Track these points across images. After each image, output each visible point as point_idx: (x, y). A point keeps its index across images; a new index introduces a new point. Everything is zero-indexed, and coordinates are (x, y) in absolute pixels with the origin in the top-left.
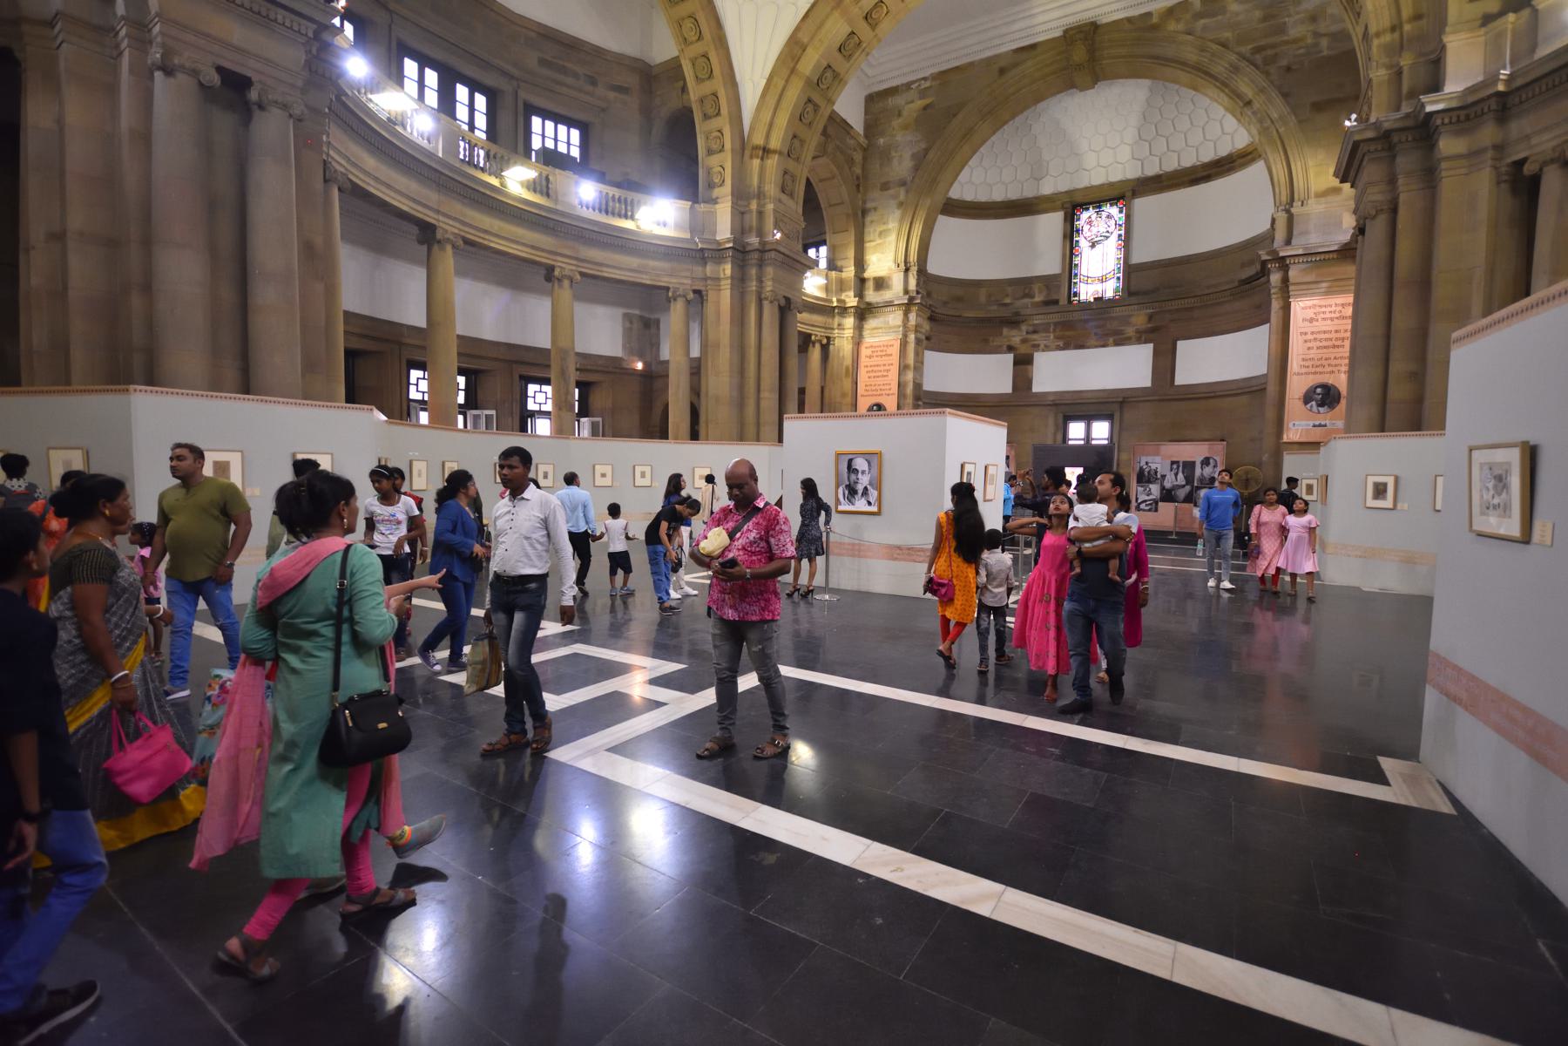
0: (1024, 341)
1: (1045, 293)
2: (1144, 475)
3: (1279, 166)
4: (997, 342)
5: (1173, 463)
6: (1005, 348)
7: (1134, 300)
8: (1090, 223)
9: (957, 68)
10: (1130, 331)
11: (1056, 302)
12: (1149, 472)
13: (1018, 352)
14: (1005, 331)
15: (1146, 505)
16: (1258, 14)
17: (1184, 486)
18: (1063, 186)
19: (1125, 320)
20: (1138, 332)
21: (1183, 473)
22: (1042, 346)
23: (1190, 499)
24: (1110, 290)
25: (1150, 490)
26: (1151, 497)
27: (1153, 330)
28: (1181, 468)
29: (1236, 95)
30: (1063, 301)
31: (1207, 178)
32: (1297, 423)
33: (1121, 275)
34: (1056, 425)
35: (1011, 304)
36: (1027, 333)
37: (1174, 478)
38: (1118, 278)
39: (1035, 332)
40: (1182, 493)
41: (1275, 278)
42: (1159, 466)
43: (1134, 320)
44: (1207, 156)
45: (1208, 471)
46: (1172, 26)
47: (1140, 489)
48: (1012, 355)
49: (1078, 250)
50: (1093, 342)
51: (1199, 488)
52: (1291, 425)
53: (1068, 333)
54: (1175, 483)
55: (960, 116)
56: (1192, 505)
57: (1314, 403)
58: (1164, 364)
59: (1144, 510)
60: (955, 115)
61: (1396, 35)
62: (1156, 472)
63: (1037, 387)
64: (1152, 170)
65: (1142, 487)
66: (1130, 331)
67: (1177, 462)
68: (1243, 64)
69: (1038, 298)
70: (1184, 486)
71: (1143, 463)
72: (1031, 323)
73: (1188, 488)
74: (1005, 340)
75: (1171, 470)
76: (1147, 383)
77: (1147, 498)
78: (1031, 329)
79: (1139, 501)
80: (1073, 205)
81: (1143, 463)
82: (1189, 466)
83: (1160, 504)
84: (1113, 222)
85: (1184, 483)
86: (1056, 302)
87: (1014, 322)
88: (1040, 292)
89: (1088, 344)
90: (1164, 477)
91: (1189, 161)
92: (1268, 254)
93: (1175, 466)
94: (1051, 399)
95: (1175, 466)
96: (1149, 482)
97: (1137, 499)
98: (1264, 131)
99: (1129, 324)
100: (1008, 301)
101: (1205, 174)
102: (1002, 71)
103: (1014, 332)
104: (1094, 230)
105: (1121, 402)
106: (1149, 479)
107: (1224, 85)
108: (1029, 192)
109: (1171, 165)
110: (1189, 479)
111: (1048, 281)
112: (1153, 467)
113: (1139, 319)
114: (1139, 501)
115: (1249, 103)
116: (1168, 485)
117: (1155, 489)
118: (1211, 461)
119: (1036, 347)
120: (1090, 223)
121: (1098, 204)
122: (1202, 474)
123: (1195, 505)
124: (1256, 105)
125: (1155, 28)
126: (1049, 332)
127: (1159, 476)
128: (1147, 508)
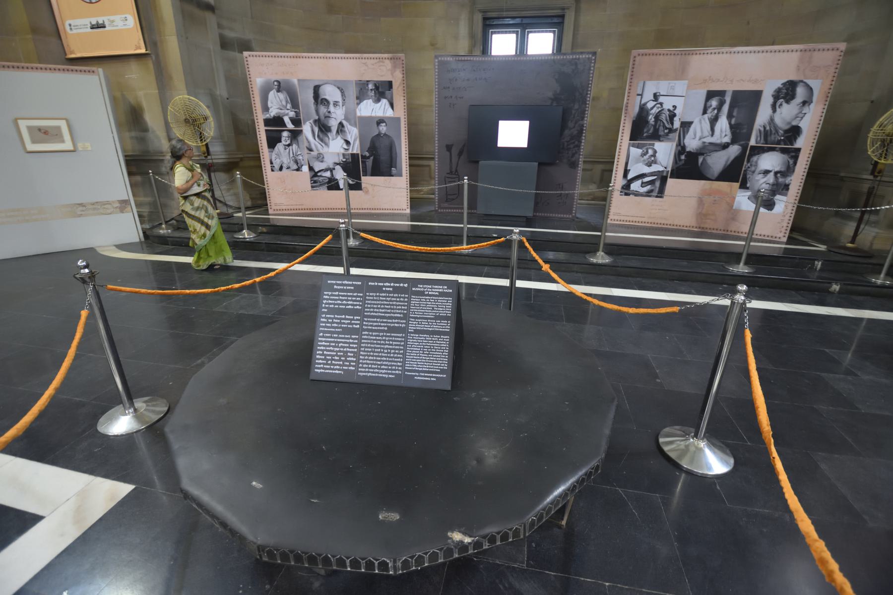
2: (647, 122)
5: (711, 95)
12: (657, 117)
15: (643, 185)
17: (725, 146)
21: (730, 116)
25: (655, 152)
26: (655, 168)
28: (726, 108)
34: (472, 36)
37: (707, 125)
40: (718, 162)
42: (679, 102)
45: (786, 113)
47: (635, 152)
51: (757, 151)
56: (737, 185)
59: (637, 194)
62: (672, 116)
65: (638, 147)
67: (721, 94)
70: (725, 146)
71: (648, 96)
75: (705, 112)
77: (646, 170)
79: (630, 176)
83: (670, 182)
85: (727, 139)
90: (686, 125)
93: (714, 103)
95: (714, 103)
97: (626, 172)
106: (656, 130)
110: (739, 133)
112: (668, 103)
114: (630, 176)
116: (692, 143)
118: (800, 91)
122: (772, 120)
123: (744, 186)
127: (677, 124)
128: (648, 188)
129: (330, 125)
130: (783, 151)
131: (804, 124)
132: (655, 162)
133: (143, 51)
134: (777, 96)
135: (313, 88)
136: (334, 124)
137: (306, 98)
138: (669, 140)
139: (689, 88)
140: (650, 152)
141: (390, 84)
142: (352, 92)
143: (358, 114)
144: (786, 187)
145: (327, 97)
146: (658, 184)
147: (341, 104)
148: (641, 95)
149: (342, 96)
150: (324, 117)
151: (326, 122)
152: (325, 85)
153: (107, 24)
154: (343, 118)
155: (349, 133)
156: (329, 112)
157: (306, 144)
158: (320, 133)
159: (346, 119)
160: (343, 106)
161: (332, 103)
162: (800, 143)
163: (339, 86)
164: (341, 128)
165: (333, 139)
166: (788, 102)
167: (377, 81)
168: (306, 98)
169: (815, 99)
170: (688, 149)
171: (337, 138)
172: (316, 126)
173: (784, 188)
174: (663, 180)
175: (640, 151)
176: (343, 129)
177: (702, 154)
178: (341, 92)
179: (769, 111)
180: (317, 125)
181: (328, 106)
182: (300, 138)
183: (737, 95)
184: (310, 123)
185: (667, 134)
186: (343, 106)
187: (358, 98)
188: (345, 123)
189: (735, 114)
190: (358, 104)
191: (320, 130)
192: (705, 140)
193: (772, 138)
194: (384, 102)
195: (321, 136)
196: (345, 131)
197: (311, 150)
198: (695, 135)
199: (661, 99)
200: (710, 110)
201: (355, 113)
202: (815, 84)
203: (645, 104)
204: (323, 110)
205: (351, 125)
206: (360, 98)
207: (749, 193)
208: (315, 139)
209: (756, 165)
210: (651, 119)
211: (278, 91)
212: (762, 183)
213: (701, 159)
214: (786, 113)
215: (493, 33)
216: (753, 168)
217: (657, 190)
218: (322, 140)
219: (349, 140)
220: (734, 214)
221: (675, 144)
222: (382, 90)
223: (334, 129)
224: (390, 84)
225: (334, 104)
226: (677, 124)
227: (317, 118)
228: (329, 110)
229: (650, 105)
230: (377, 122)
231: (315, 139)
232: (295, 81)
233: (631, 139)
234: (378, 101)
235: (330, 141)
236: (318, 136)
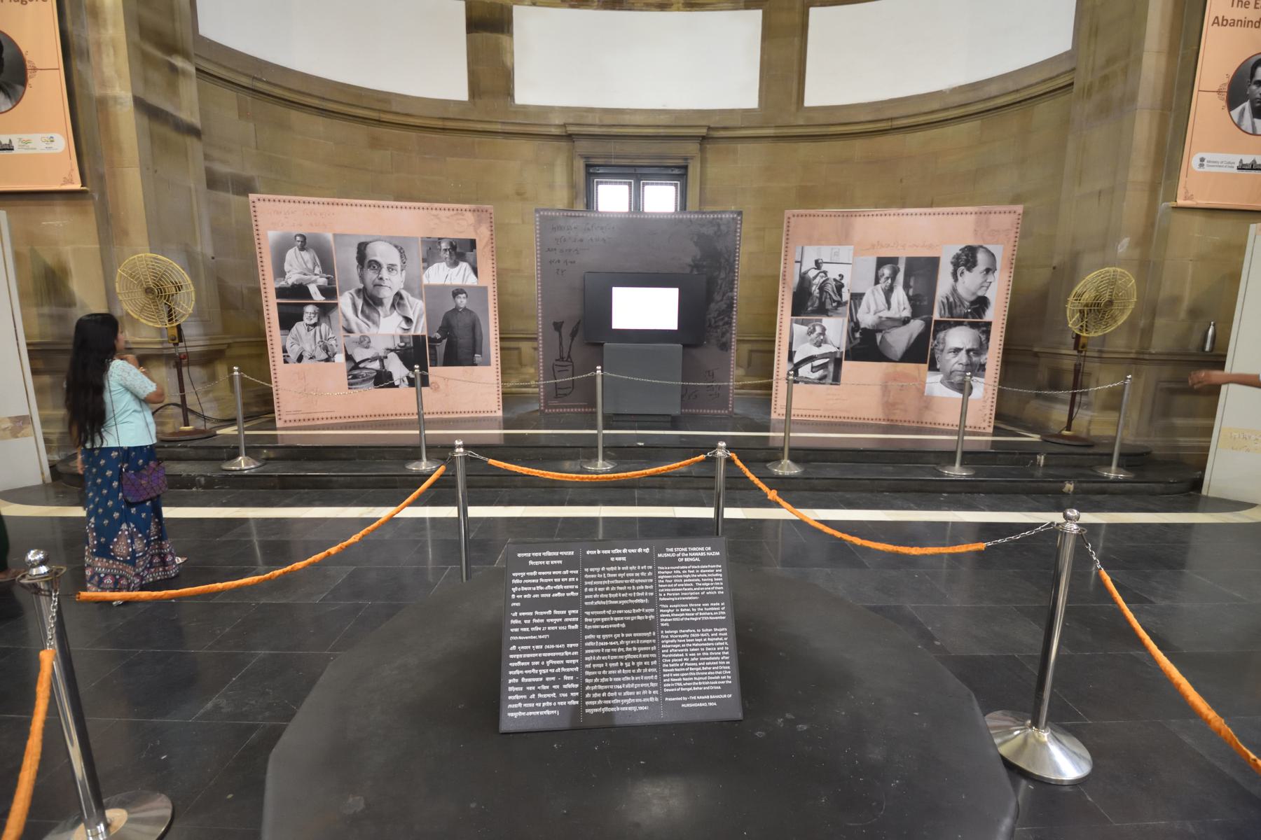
2: (810, 294)
5: (881, 262)
15: (814, 369)
17: (905, 321)
21: (906, 286)
23: (920, 352)
25: (824, 329)
26: (825, 349)
28: (900, 277)
32: (1208, 156)
34: (572, 186)
37: (881, 298)
40: (899, 339)
42: (846, 271)
45: (969, 283)
47: (800, 330)
51: (943, 326)
52: (1195, 162)
54: (885, 314)
56: (925, 366)
57: (1247, 105)
59: (807, 381)
62: (840, 287)
65: (803, 323)
67: (893, 261)
70: (905, 321)
71: (808, 264)
73: (917, 326)
75: (877, 282)
77: (816, 351)
79: (796, 360)
81: (808, 264)
83: (847, 366)
85: (907, 313)
90: (857, 297)
93: (886, 271)
95: (886, 271)
96: (822, 311)
97: (791, 358)
106: (822, 304)
110: (920, 305)
112: (833, 272)
116: (867, 319)
117: (835, 329)
118: (981, 257)
122: (954, 290)
123: (933, 367)
127: (846, 297)
129: (380, 297)
130: (973, 325)
131: (991, 294)
132: (825, 341)
133: (77, 186)
134: (956, 263)
135: (356, 246)
136: (387, 295)
137: (346, 259)
138: (839, 315)
139: (855, 254)
140: (818, 330)
141: (472, 244)
142: (416, 253)
143: (425, 281)
144: (982, 367)
145: (378, 259)
146: (831, 368)
147: (399, 268)
148: (801, 262)
149: (401, 257)
150: (372, 286)
151: (375, 293)
152: (374, 243)
153: (15, 144)
154: (402, 287)
155: (411, 307)
156: (381, 279)
157: (343, 323)
158: (365, 308)
159: (407, 288)
160: (402, 270)
161: (385, 267)
162: (989, 315)
163: (397, 243)
164: (398, 300)
165: (386, 316)
166: (969, 269)
167: (453, 239)
168: (346, 259)
169: (998, 265)
170: (862, 326)
171: (391, 314)
172: (359, 297)
173: (980, 369)
174: (838, 363)
175: (805, 329)
176: (401, 302)
177: (881, 331)
178: (400, 252)
179: (951, 280)
180: (362, 296)
181: (380, 271)
182: (333, 315)
183: (913, 263)
184: (351, 294)
185: (836, 308)
186: (402, 270)
187: (424, 260)
188: (404, 293)
189: (912, 283)
190: (425, 268)
191: (366, 302)
192: (881, 314)
193: (958, 311)
194: (464, 266)
195: (367, 311)
196: (404, 305)
197: (349, 331)
198: (869, 309)
199: (824, 267)
200: (882, 280)
201: (421, 280)
202: (997, 250)
203: (806, 273)
204: (371, 275)
205: (413, 295)
206: (428, 260)
207: (939, 377)
208: (357, 316)
209: (944, 343)
210: (815, 290)
211: (302, 248)
212: (954, 363)
213: (879, 337)
215: (598, 183)
216: (941, 347)
217: (831, 375)
218: (368, 317)
219: (411, 316)
220: (927, 402)
221: (846, 320)
222: (461, 251)
223: (388, 302)
224: (472, 244)
225: (388, 268)
226: (846, 297)
227: (361, 286)
228: (380, 276)
229: (812, 274)
230: (453, 292)
231: (357, 316)
232: (330, 236)
233: (793, 315)
234: (455, 264)
235: (381, 318)
236: (363, 312)
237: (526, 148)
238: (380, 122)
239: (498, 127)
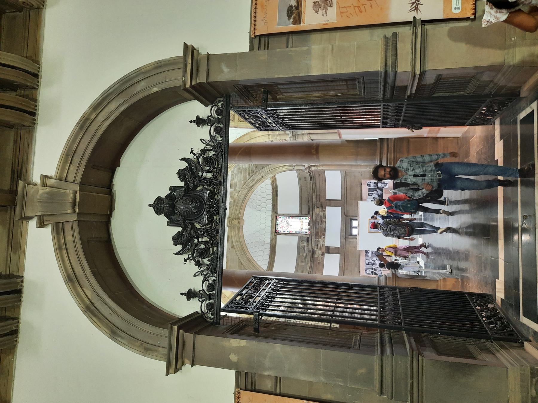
0: (320, 249)
1: (304, 242)
3: (282, 169)
4: (320, 259)
5: (369, 195)
6: (322, 256)
7: (311, 212)
8: (282, 227)
9: (226, 263)
10: (321, 214)
11: (308, 238)
13: (324, 252)
14: (316, 256)
16: (239, 175)
17: (377, 192)
18: (269, 235)
19: (317, 215)
20: (322, 211)
22: (323, 243)
24: (306, 221)
27: (322, 206)
29: (259, 180)
30: (308, 236)
31: (277, 192)
33: (301, 218)
34: (353, 238)
35: (306, 254)
36: (318, 248)
38: (302, 218)
39: (318, 245)
40: (380, 192)
41: (313, 168)
43: (318, 213)
44: (270, 191)
46: (235, 196)
48: (325, 254)
49: (291, 232)
50: (323, 226)
51: (378, 187)
53: (319, 234)
55: (243, 262)
58: (333, 203)
60: (242, 264)
61: (270, 135)
63: (339, 245)
64: (270, 207)
66: (321, 214)
67: (369, 194)
68: (252, 178)
69: (305, 244)
70: (377, 192)
72: (314, 247)
74: (319, 256)
76: (340, 208)
78: (316, 247)
80: (276, 233)
82: (370, 190)
84: (284, 220)
85: (376, 191)
86: (308, 238)
87: (313, 253)
88: (303, 243)
89: (324, 227)
90: (374, 198)
91: (270, 197)
92: (306, 170)
93: (370, 194)
94: (343, 240)
98: (271, 173)
99: (319, 214)
100: (305, 255)
101: (275, 192)
102: (233, 247)
103: (317, 253)
104: (285, 226)
105: (346, 216)
107: (256, 183)
108: (268, 247)
109: (270, 202)
110: (375, 190)
111: (300, 241)
113: (318, 211)
115: (262, 177)
118: (368, 184)
119: (323, 245)
120: (282, 227)
121: (276, 225)
123: (384, 188)
124: (263, 175)
125: (234, 201)
126: (318, 241)
130: (378, 183)
131: (374, 182)
137: (368, 266)
142: (367, 258)
206: (368, 256)
214: (372, 184)
237: (347, 246)
238: (344, 268)
239: (344, 250)
